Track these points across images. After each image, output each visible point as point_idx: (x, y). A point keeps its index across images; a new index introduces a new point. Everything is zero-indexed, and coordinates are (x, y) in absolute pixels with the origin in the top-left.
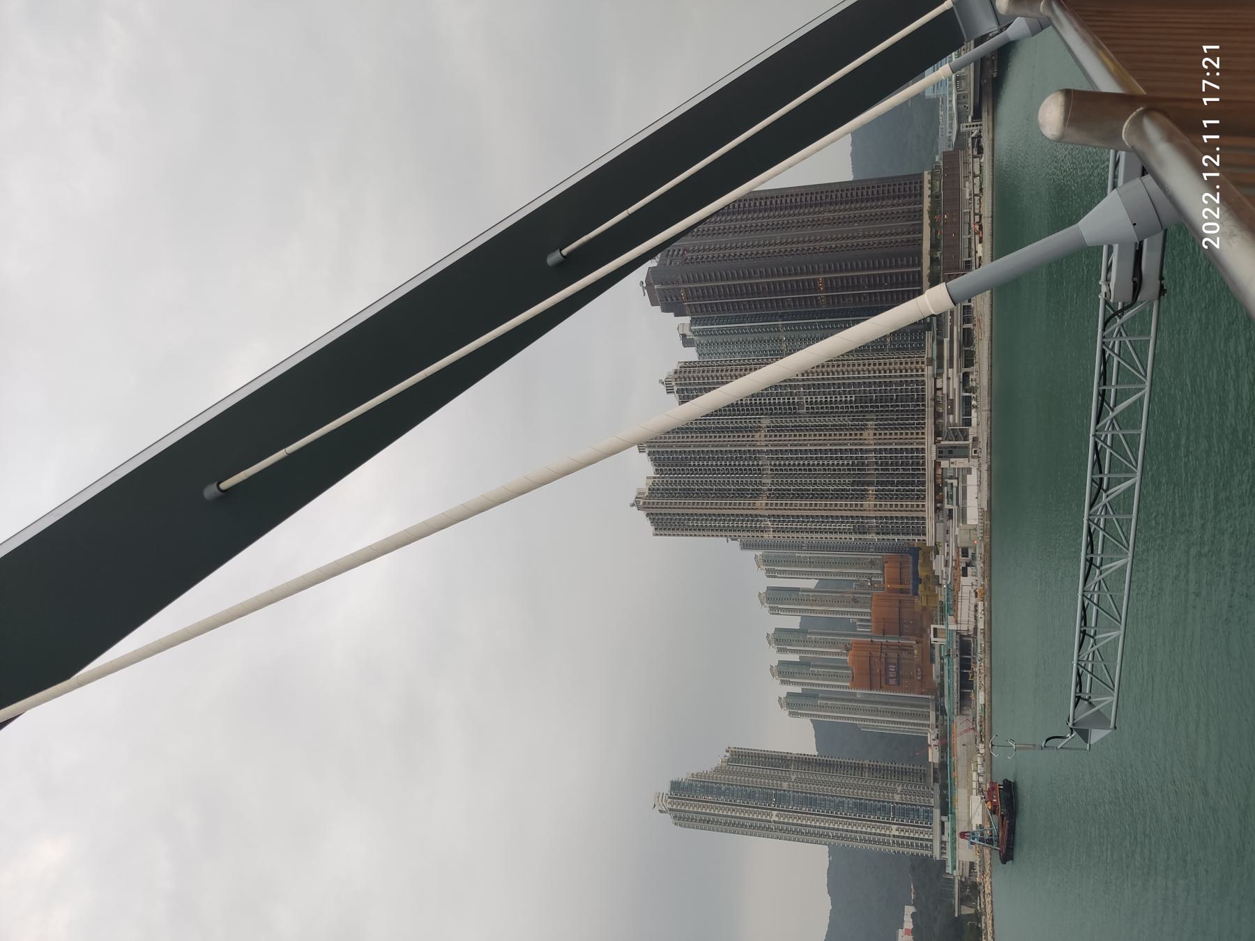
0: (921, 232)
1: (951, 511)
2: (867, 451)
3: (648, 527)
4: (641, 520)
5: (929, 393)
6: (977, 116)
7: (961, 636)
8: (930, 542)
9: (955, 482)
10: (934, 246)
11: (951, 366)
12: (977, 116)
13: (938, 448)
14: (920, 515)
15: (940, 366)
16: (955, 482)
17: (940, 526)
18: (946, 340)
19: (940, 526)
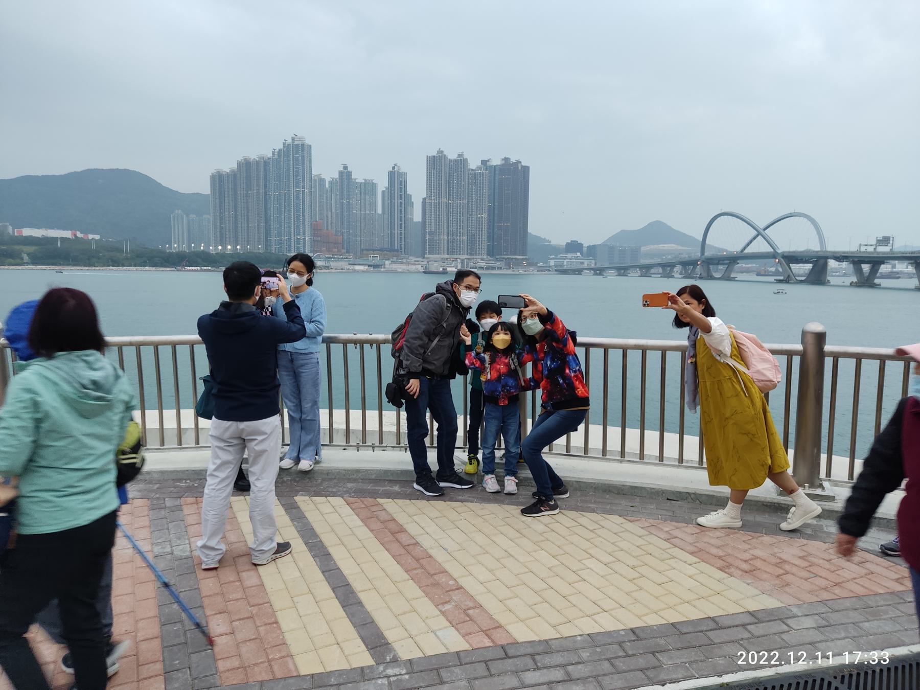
0: (519, 255)
1: (445, 263)
2: (460, 237)
3: (430, 155)
4: (435, 153)
5: (475, 257)
6: (556, 270)
7: (381, 265)
8: (426, 256)
9: (454, 264)
10: (515, 259)
11: (486, 263)
12: (556, 270)
13: (464, 259)
14: (442, 253)
15: (486, 261)
16: (454, 264)
17: (440, 259)
18: (493, 262)
19: (440, 259)
